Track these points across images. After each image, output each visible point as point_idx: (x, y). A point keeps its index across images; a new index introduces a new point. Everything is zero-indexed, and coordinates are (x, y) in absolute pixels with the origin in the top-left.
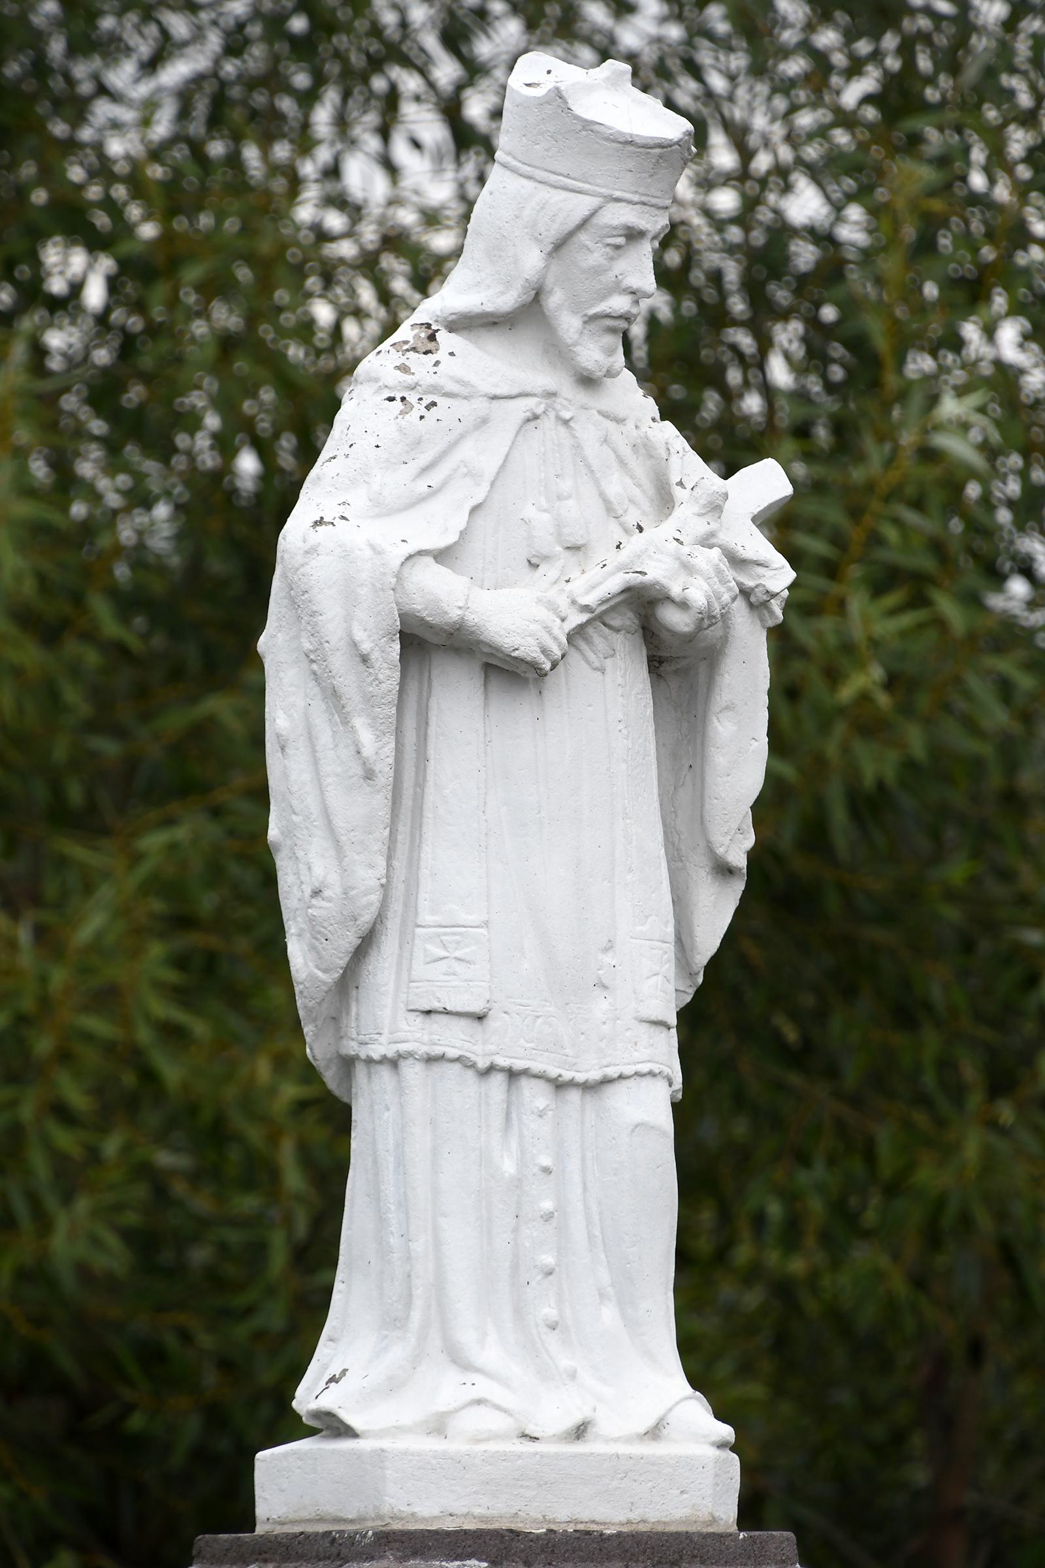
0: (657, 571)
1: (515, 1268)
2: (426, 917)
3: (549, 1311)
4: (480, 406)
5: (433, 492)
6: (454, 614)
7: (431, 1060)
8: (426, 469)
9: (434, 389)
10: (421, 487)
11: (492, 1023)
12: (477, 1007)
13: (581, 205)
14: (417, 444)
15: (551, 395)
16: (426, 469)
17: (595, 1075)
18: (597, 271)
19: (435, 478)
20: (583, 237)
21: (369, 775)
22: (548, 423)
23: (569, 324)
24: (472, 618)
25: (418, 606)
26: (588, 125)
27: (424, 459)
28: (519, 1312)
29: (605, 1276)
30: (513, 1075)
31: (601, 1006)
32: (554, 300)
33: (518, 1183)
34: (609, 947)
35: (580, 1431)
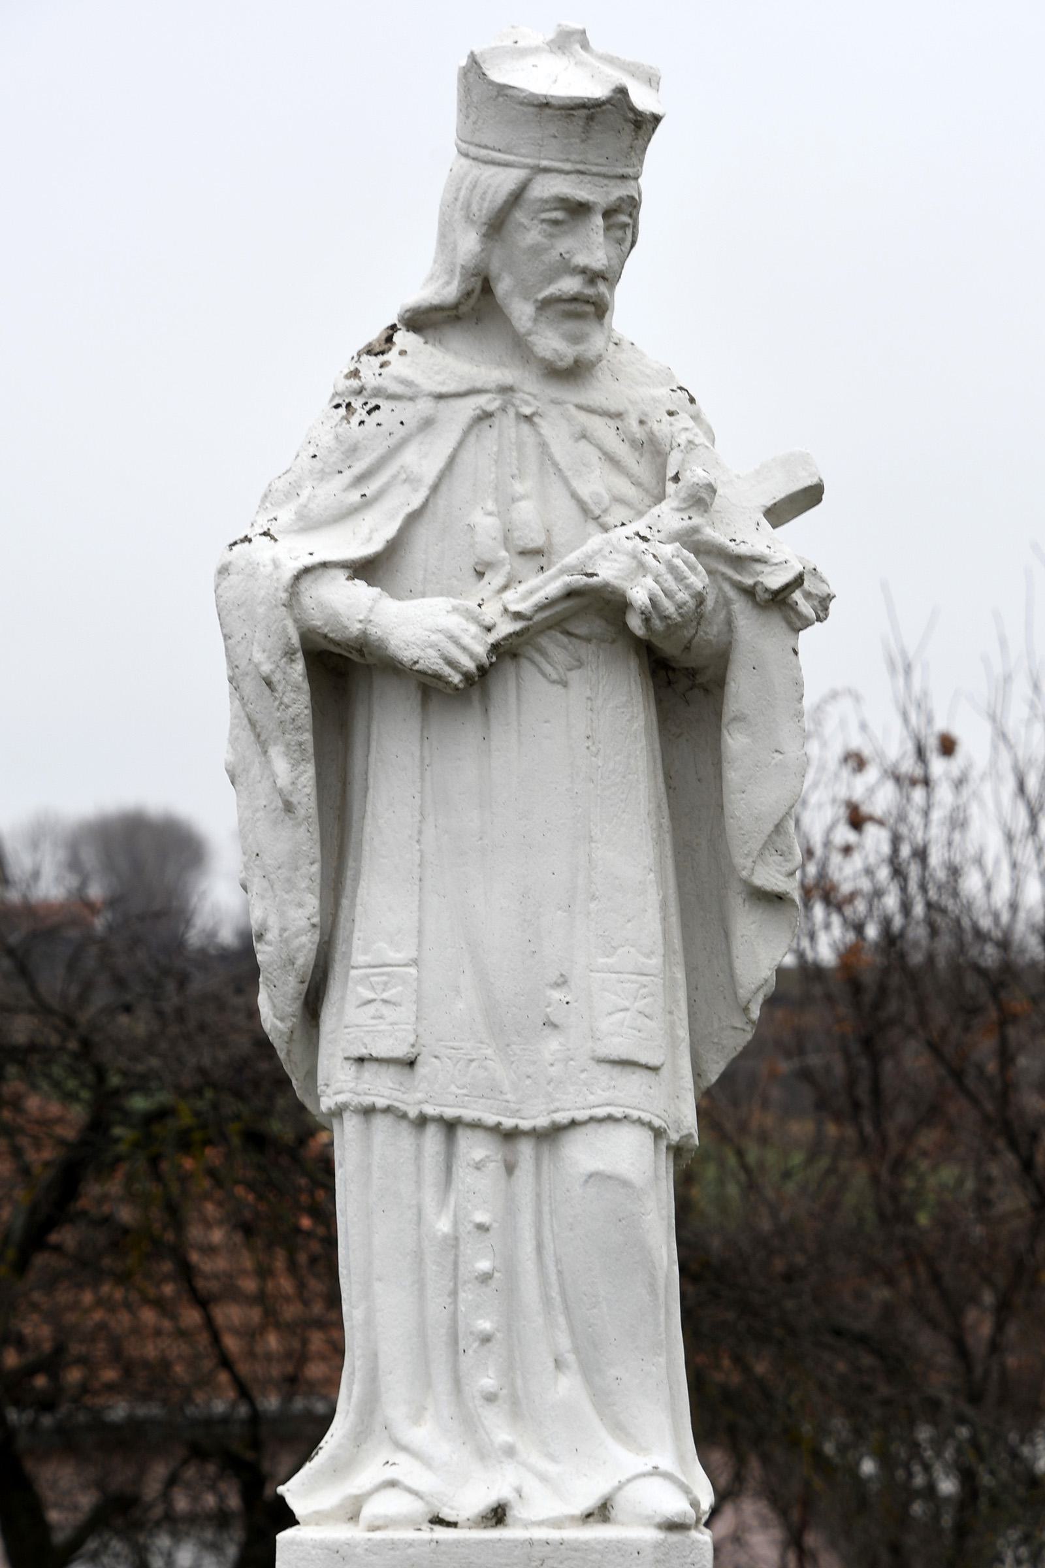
0: (608, 572)
1: (454, 1339)
2: (358, 958)
3: (488, 1382)
4: (424, 406)
5: (367, 502)
6: (355, 628)
7: (368, 1112)
8: (361, 479)
9: (378, 392)
10: (354, 497)
11: (421, 1069)
12: (401, 1051)
13: (508, 179)
14: (353, 451)
15: (506, 390)
16: (361, 479)
17: (542, 1122)
18: (536, 251)
19: (371, 488)
20: (520, 216)
21: (289, 807)
22: (507, 422)
23: (521, 312)
24: (375, 631)
25: (317, 621)
26: (503, 90)
27: (359, 467)
28: (457, 1383)
29: (564, 1342)
30: (451, 1126)
31: (553, 1045)
32: (503, 287)
33: (453, 1242)
34: (562, 982)
35: (498, 1515)
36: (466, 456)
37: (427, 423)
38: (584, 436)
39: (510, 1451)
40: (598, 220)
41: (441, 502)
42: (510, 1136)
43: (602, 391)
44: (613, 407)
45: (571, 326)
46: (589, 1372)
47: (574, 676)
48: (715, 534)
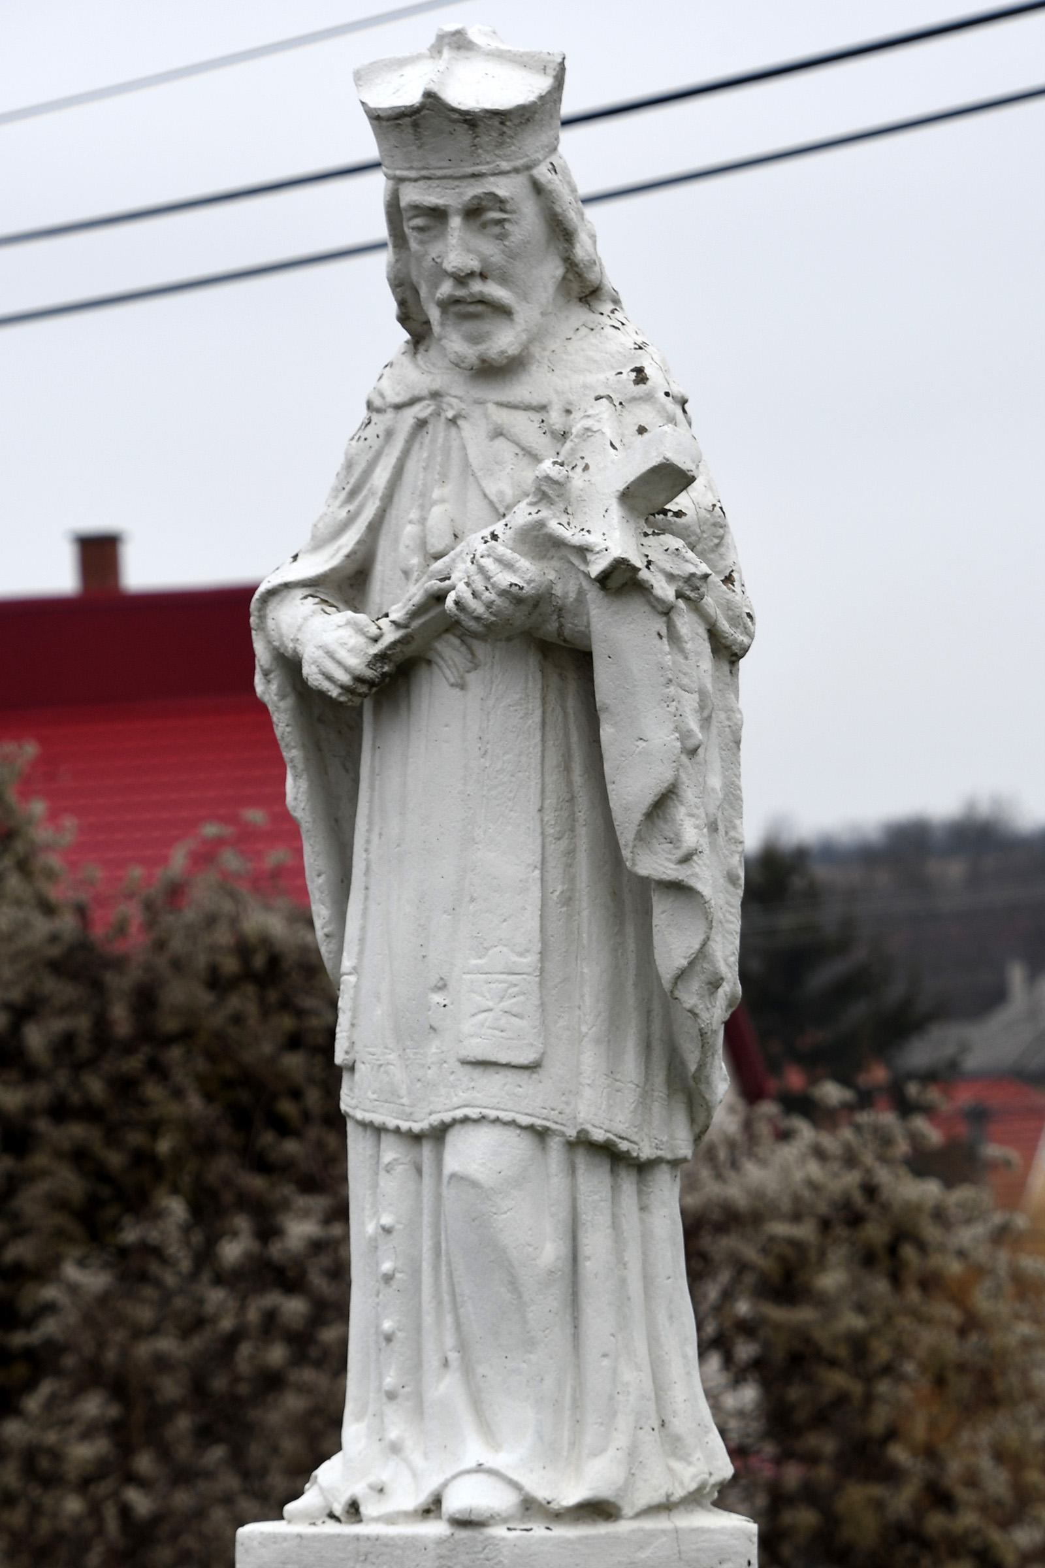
15: (435, 395)
29: (450, 1340)
34: (442, 987)
36: (413, 467)
37: (389, 434)
38: (498, 433)
39: (395, 1449)
40: (456, 222)
41: (393, 514)
42: (416, 1138)
43: (523, 390)
44: (536, 400)
45: (469, 326)
46: (468, 1371)
47: (471, 678)
48: (554, 527)
